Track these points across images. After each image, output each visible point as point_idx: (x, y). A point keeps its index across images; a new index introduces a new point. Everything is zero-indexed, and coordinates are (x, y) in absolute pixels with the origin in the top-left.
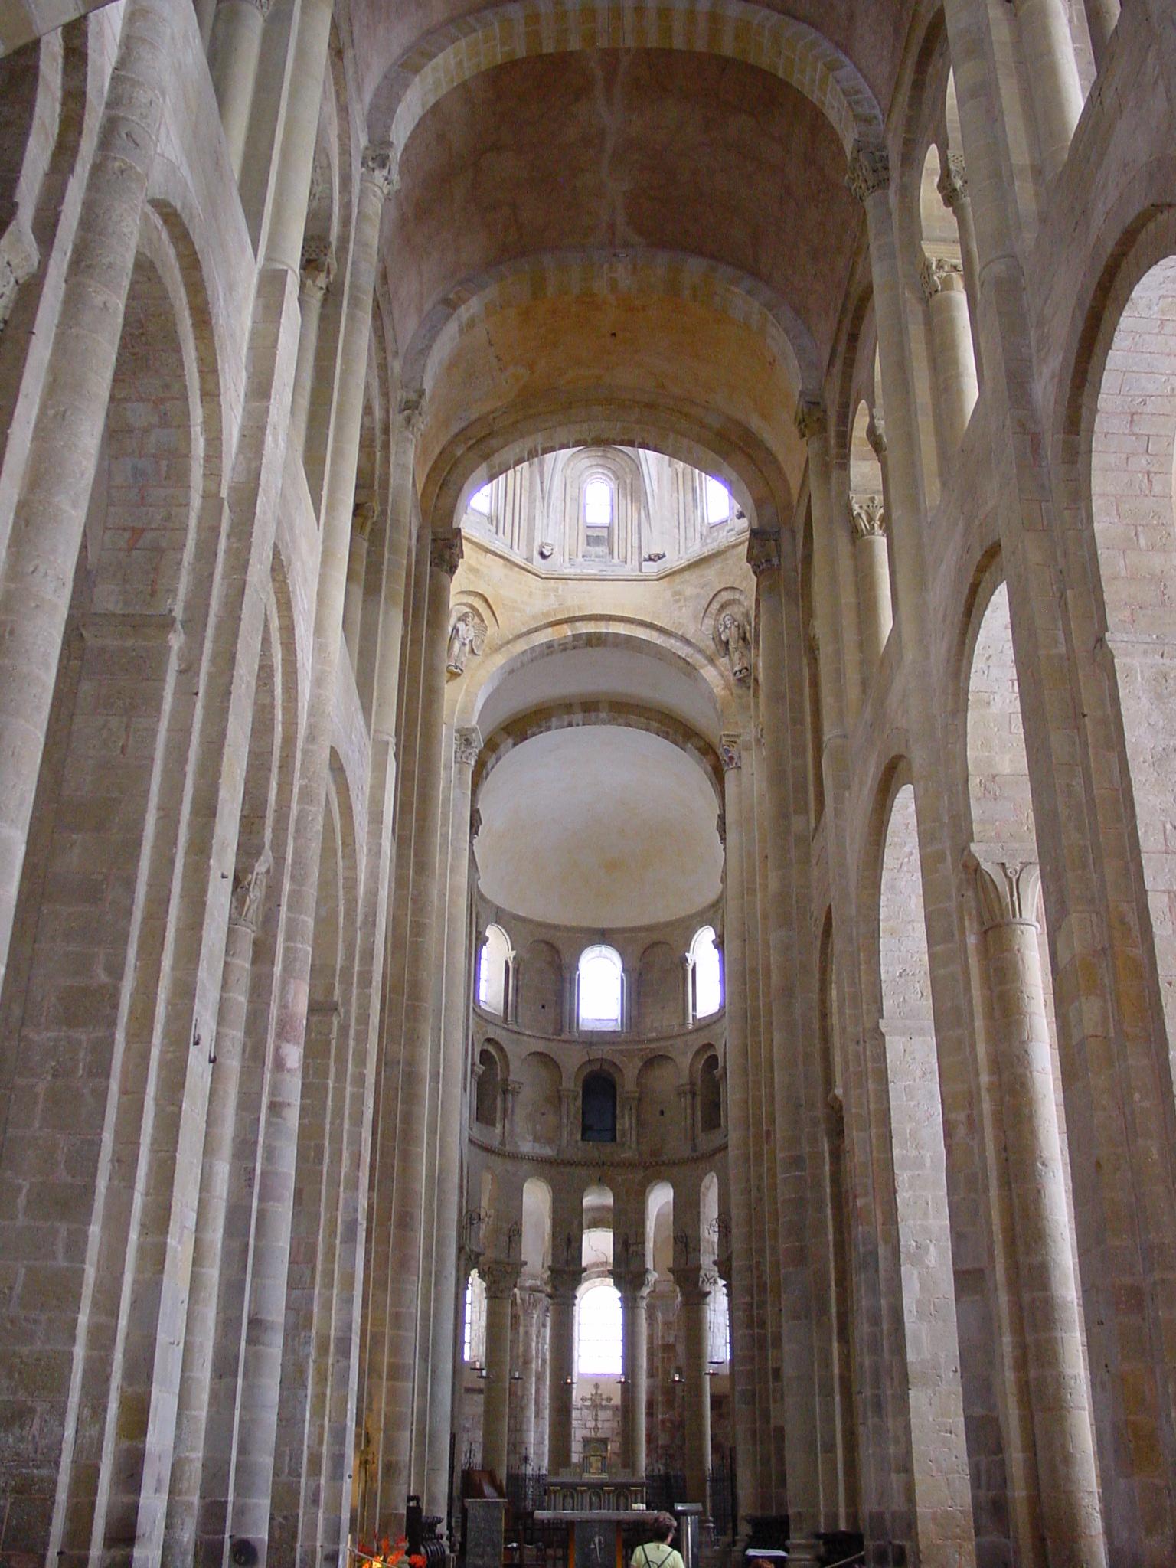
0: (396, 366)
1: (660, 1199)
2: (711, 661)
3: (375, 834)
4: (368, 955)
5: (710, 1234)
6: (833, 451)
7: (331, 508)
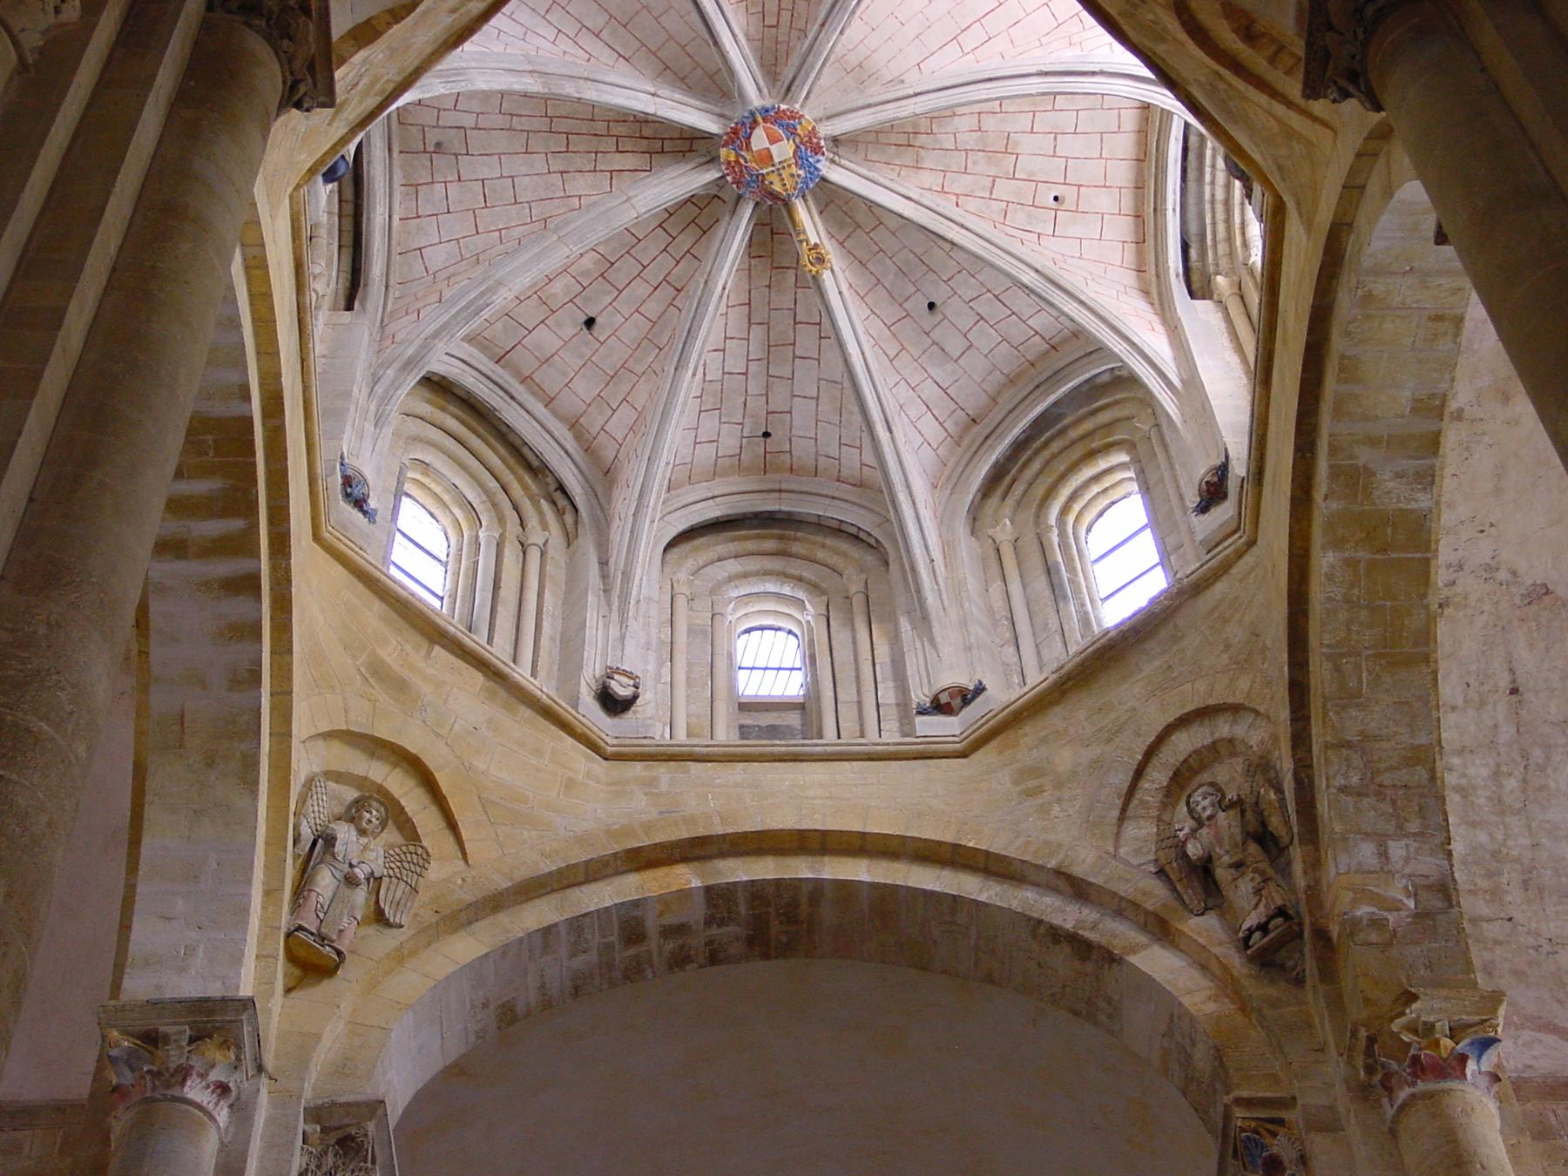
2: (1161, 929)
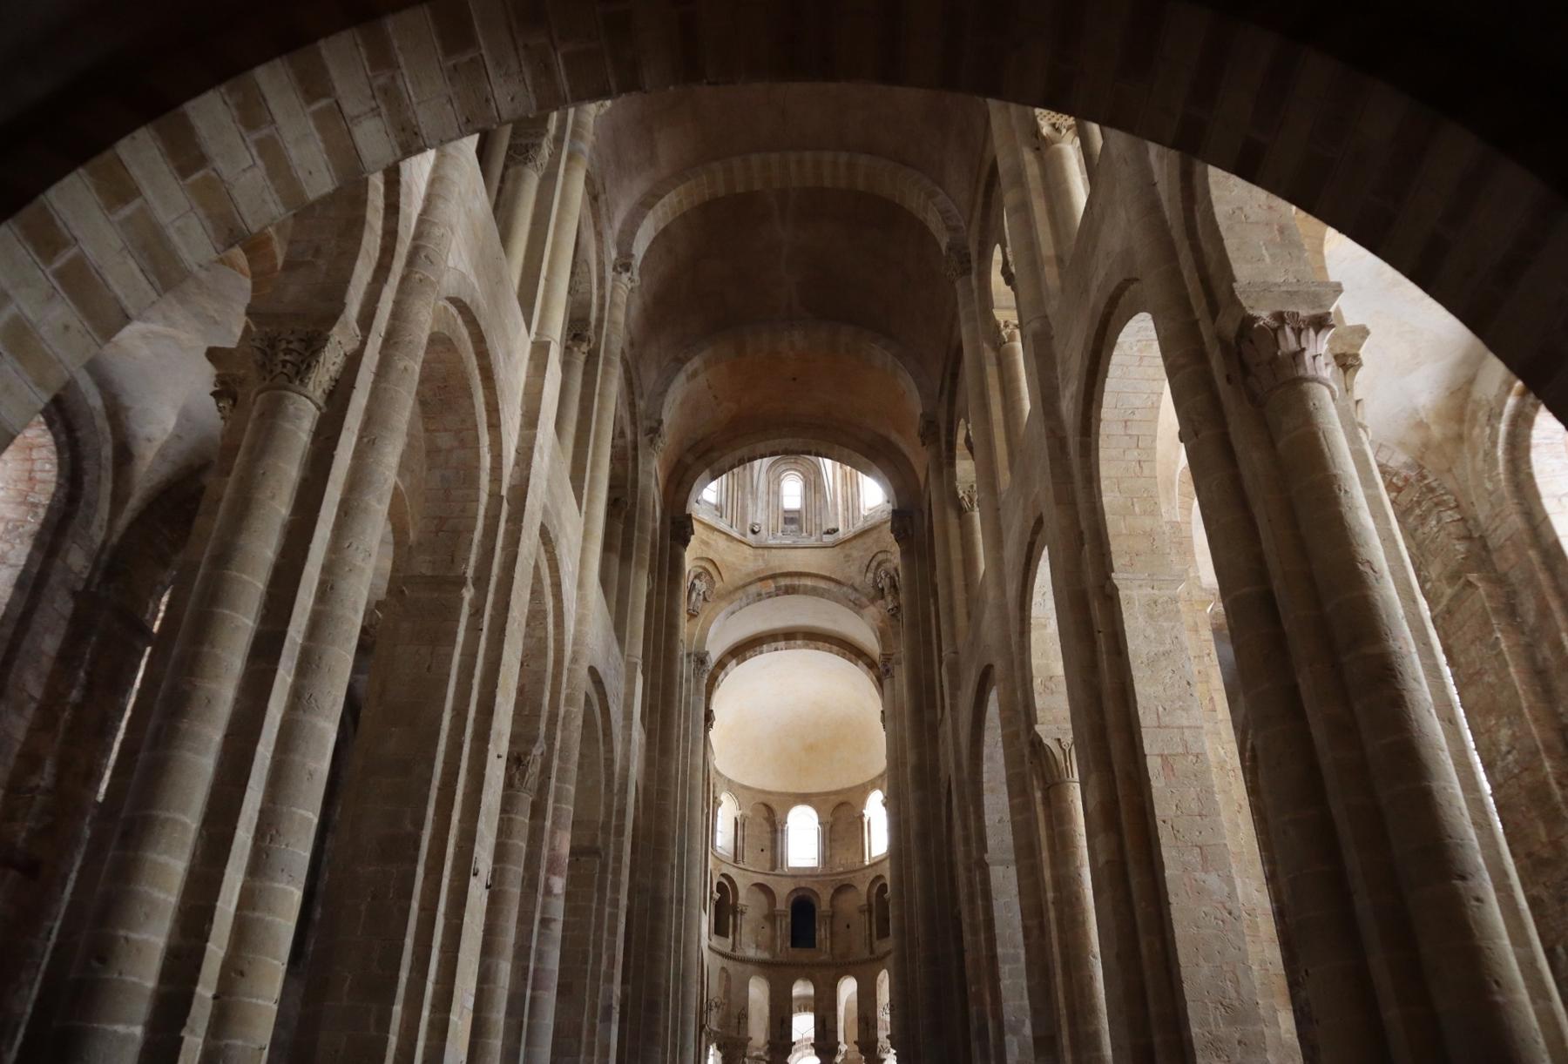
0: (642, 405)
1: (848, 989)
2: (873, 601)
3: (628, 726)
4: (622, 813)
5: (884, 1017)
6: (944, 454)
7: (590, 501)
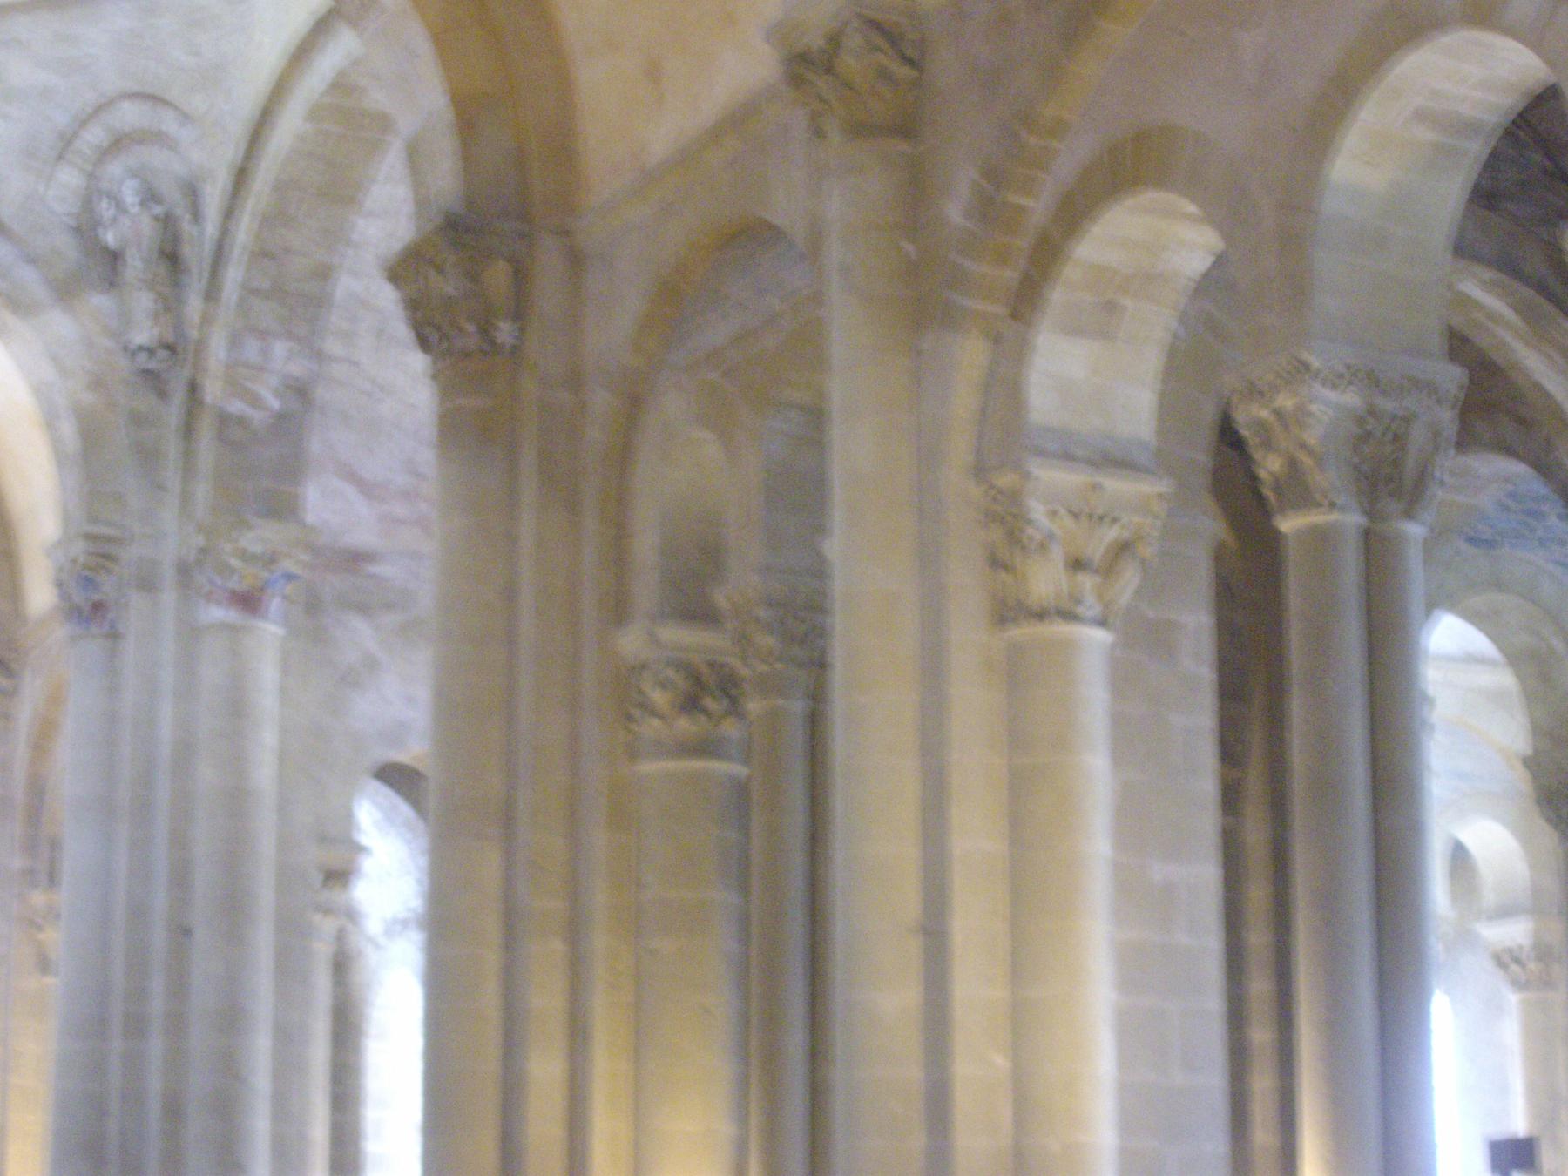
2: (66, 291)
